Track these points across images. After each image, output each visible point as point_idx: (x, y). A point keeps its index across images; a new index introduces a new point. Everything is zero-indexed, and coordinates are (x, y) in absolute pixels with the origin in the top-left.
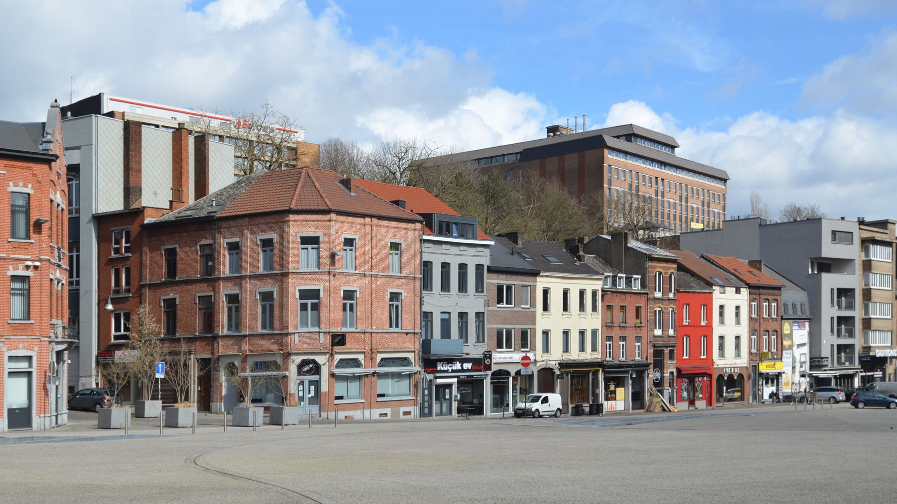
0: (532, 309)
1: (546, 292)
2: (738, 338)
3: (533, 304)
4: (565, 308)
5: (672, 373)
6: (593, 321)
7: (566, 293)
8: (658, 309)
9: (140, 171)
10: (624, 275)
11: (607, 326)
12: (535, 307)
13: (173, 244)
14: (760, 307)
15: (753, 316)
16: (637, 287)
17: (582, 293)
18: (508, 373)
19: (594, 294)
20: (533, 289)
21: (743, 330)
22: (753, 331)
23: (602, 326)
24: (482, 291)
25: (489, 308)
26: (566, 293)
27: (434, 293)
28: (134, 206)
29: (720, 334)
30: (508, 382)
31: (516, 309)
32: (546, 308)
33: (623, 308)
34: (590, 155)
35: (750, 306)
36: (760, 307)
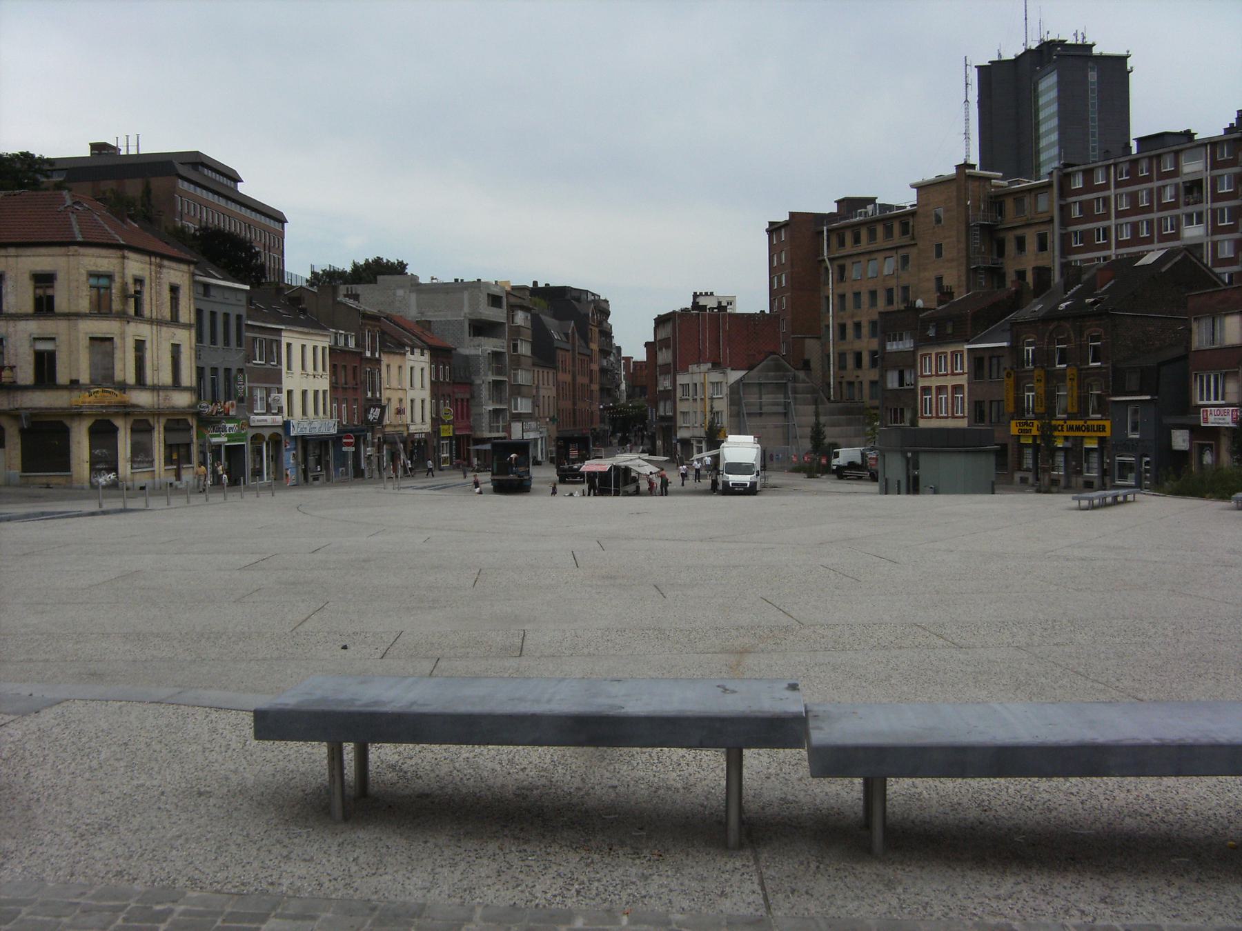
1: (289, 345)
3: (279, 362)
5: (379, 438)
7: (303, 347)
8: (368, 369)
12: (281, 365)
16: (352, 344)
17: (315, 348)
18: (262, 437)
19: (324, 349)
20: (279, 343)
21: (426, 394)
22: (434, 395)
26: (303, 347)
31: (268, 366)
32: (289, 368)
33: (345, 367)
34: (157, 183)
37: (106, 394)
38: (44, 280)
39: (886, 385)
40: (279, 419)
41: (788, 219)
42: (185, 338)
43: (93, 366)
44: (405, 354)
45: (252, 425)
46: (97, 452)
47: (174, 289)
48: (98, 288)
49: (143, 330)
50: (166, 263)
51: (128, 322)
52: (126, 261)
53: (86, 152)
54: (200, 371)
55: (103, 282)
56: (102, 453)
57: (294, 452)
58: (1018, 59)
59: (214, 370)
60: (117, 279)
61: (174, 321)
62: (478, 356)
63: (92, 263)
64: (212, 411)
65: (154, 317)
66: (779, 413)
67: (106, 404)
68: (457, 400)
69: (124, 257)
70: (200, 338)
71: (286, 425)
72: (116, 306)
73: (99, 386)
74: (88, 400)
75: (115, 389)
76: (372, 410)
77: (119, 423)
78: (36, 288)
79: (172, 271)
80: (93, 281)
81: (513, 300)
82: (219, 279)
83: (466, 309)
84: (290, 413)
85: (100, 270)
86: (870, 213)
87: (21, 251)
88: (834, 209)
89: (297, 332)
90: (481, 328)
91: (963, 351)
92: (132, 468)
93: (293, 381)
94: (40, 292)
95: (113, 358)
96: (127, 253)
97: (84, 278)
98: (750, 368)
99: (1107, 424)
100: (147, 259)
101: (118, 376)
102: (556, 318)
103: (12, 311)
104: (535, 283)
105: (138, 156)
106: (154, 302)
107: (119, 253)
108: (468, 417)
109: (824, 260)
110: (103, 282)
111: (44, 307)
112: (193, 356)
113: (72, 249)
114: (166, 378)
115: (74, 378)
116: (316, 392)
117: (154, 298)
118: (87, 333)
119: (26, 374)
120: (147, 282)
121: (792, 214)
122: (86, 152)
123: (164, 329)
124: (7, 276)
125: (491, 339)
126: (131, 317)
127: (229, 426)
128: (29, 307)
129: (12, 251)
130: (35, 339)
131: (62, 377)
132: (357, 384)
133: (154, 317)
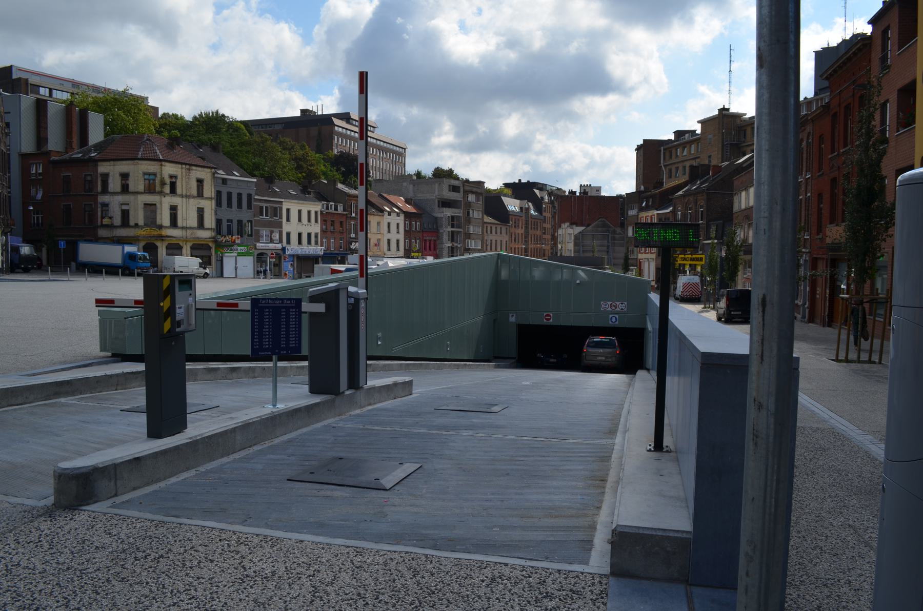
0: (280, 220)
1: (288, 210)
2: (398, 241)
3: (281, 217)
4: (300, 220)
6: (316, 228)
7: (300, 212)
9: (46, 128)
10: (333, 203)
11: (322, 230)
12: (282, 219)
14: (410, 224)
15: (407, 229)
17: (309, 212)
19: (316, 213)
20: (281, 209)
21: (401, 236)
23: (321, 231)
24: (251, 209)
25: (255, 218)
26: (300, 212)
28: (43, 150)
29: (388, 238)
30: (267, 260)
31: (271, 219)
32: (288, 220)
35: (405, 224)
36: (410, 224)
37: (152, 231)
38: (125, 176)
39: (628, 235)
40: (279, 246)
41: (642, 143)
42: (209, 206)
43: (145, 217)
44: (383, 216)
45: (257, 248)
47: (200, 182)
48: (149, 180)
49: (175, 200)
50: (194, 168)
51: (165, 196)
52: (163, 167)
53: (298, 114)
54: (219, 222)
55: (152, 177)
57: (292, 263)
58: (839, 45)
59: (229, 221)
60: (158, 176)
61: (200, 195)
62: (442, 218)
64: (222, 240)
65: (184, 193)
66: (604, 251)
67: (152, 235)
68: (425, 240)
69: (161, 165)
70: (219, 204)
71: (284, 249)
72: (158, 189)
73: (149, 226)
74: (142, 233)
75: (157, 228)
76: (353, 244)
77: (158, 244)
78: (122, 180)
79: (198, 172)
80: (146, 177)
81: (467, 188)
82: (238, 176)
83: (437, 193)
84: (288, 242)
85: (149, 171)
86: (687, 138)
87: (116, 163)
88: (672, 137)
89: (294, 203)
90: (446, 204)
91: (655, 215)
93: (291, 227)
94: (123, 182)
95: (156, 213)
96: (163, 163)
97: (141, 176)
98: (588, 226)
99: (703, 256)
100: (180, 166)
101: (158, 222)
102: (516, 198)
103: (112, 191)
104: (520, 180)
105: (322, 115)
106: (184, 187)
107: (160, 163)
108: (435, 249)
109: (661, 166)
110: (152, 177)
111: (125, 189)
112: (213, 213)
113: (136, 161)
114: (194, 222)
115: (136, 223)
116: (309, 235)
117: (184, 187)
119: (117, 221)
120: (179, 177)
121: (645, 141)
122: (298, 114)
123: (191, 200)
124: (110, 175)
125: (451, 209)
126: (167, 194)
127: (239, 248)
128: (119, 189)
129: (112, 163)
130: (121, 204)
131: (132, 223)
132: (343, 230)
133: (184, 193)
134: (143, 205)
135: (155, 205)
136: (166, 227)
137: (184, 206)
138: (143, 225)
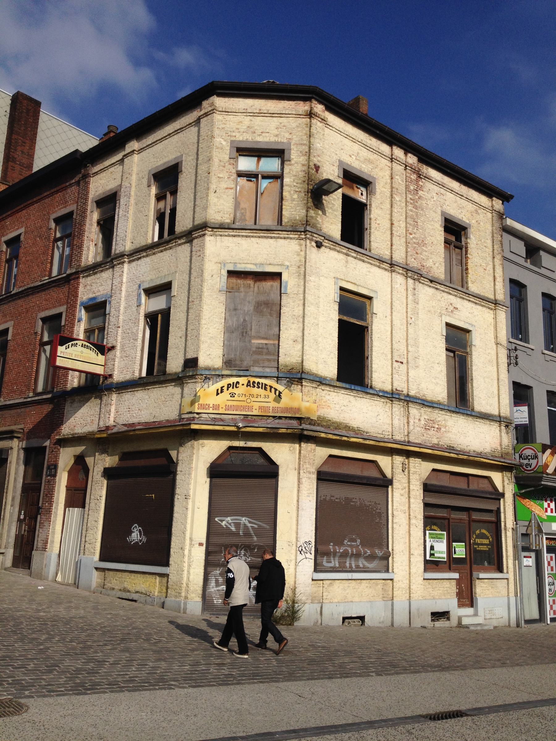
13: (18, 229)
27: (532, 347)
37: (255, 391)
46: (227, 522)
56: (237, 525)
63: (243, 128)
73: (244, 371)
75: (278, 379)
85: (259, 139)
92: (317, 569)
112: (504, 360)
115: (190, 356)
118: (223, 263)
134: (225, 273)
135: (278, 276)
136: (321, 381)
137: (399, 306)
138: (218, 363)
